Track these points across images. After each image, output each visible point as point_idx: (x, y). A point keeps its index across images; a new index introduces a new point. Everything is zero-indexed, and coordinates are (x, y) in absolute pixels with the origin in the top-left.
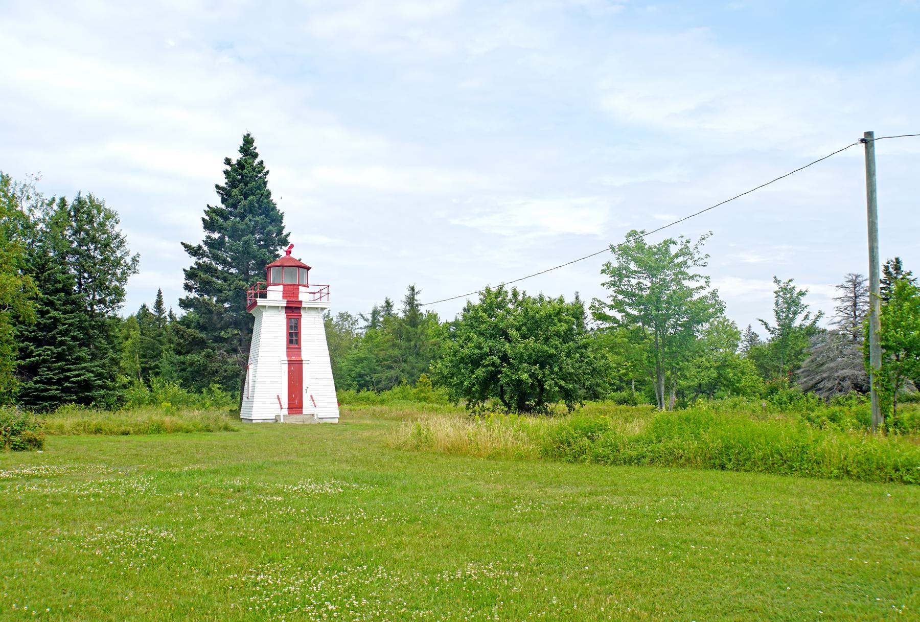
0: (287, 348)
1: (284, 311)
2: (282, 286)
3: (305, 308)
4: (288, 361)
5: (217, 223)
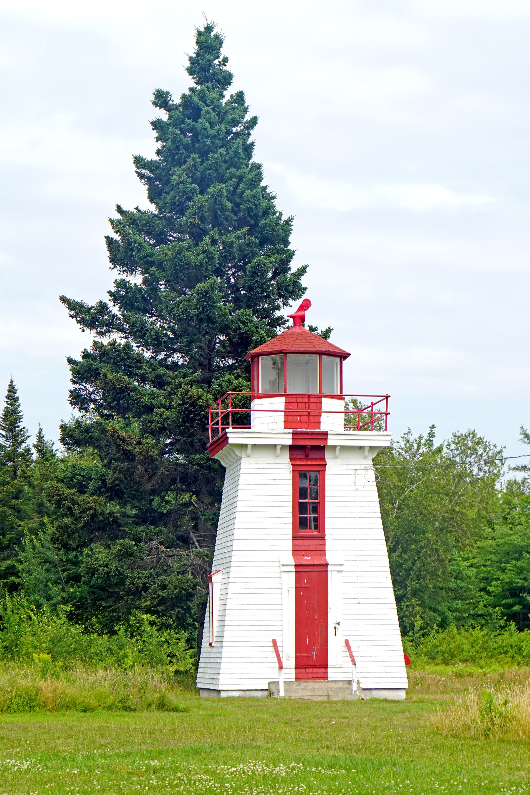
1: (287, 455)
2: (283, 399)
3: (334, 447)
4: (296, 566)
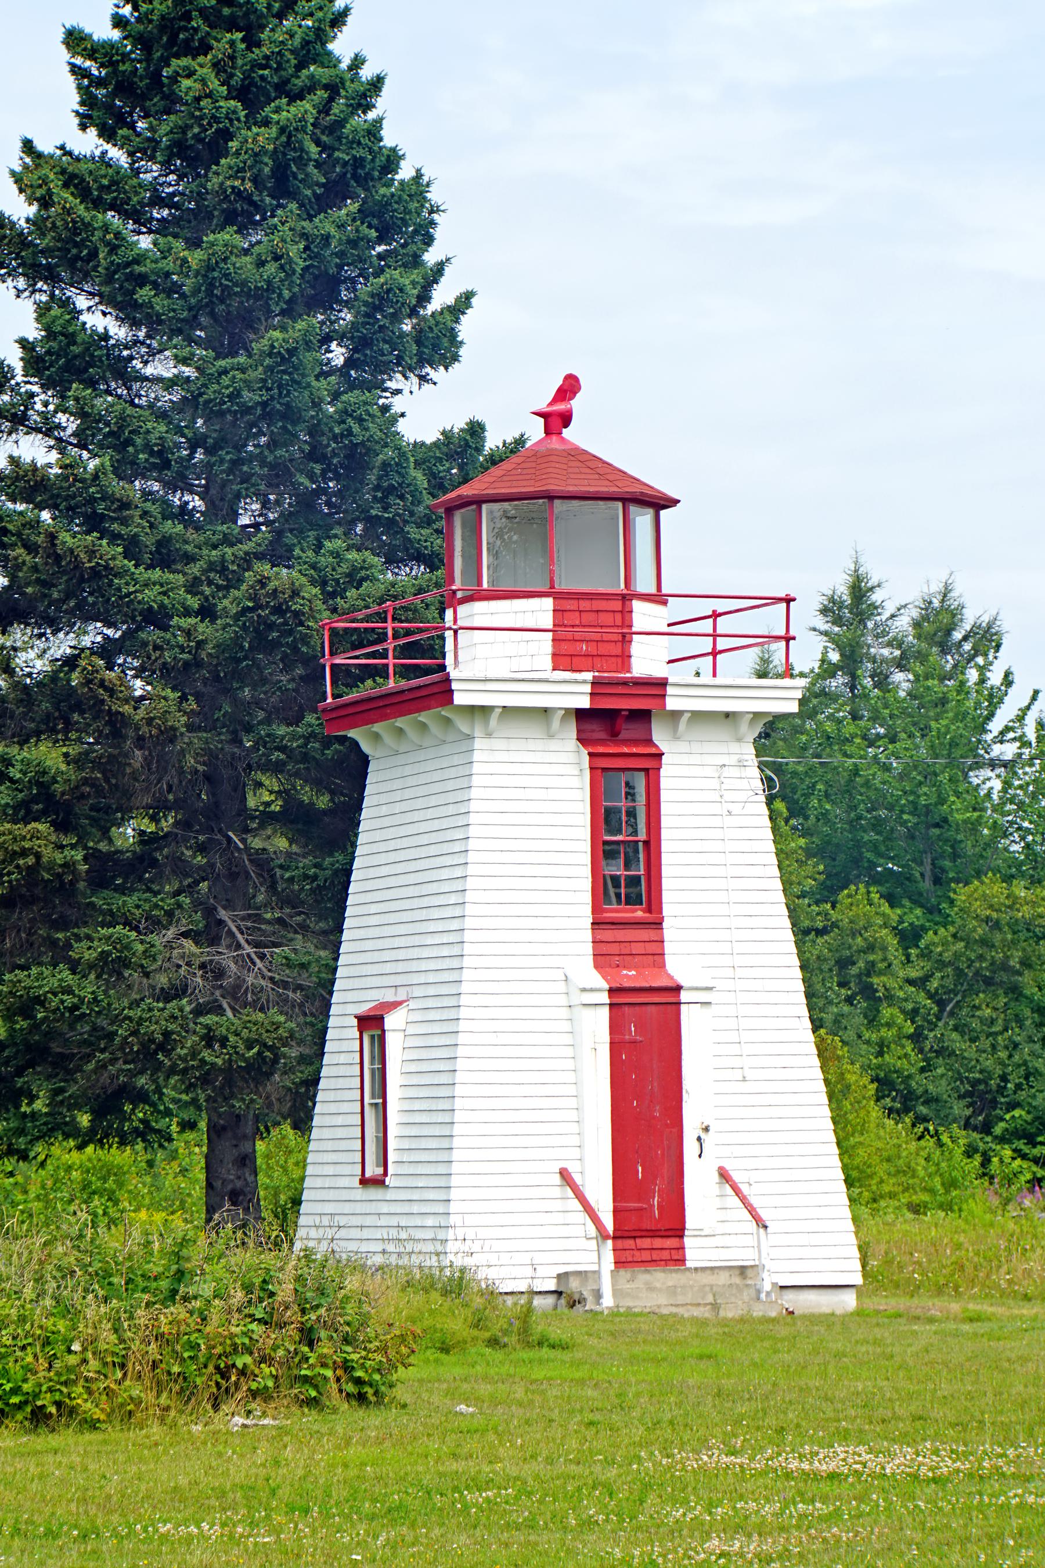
0: (597, 924)
1: (571, 731)
2: (548, 603)
3: (676, 715)
4: (611, 991)
5: (113, 249)
